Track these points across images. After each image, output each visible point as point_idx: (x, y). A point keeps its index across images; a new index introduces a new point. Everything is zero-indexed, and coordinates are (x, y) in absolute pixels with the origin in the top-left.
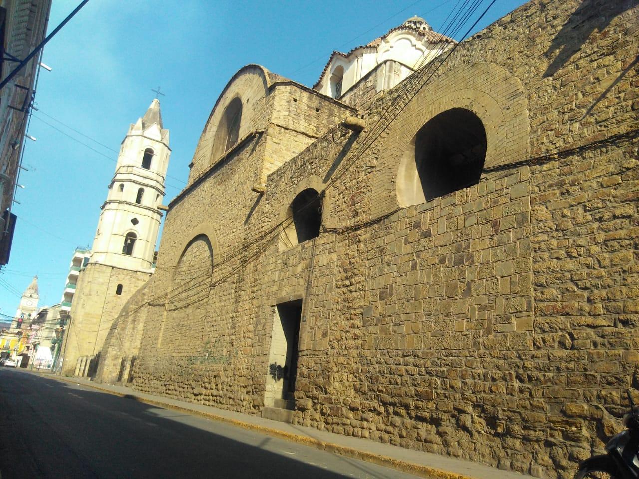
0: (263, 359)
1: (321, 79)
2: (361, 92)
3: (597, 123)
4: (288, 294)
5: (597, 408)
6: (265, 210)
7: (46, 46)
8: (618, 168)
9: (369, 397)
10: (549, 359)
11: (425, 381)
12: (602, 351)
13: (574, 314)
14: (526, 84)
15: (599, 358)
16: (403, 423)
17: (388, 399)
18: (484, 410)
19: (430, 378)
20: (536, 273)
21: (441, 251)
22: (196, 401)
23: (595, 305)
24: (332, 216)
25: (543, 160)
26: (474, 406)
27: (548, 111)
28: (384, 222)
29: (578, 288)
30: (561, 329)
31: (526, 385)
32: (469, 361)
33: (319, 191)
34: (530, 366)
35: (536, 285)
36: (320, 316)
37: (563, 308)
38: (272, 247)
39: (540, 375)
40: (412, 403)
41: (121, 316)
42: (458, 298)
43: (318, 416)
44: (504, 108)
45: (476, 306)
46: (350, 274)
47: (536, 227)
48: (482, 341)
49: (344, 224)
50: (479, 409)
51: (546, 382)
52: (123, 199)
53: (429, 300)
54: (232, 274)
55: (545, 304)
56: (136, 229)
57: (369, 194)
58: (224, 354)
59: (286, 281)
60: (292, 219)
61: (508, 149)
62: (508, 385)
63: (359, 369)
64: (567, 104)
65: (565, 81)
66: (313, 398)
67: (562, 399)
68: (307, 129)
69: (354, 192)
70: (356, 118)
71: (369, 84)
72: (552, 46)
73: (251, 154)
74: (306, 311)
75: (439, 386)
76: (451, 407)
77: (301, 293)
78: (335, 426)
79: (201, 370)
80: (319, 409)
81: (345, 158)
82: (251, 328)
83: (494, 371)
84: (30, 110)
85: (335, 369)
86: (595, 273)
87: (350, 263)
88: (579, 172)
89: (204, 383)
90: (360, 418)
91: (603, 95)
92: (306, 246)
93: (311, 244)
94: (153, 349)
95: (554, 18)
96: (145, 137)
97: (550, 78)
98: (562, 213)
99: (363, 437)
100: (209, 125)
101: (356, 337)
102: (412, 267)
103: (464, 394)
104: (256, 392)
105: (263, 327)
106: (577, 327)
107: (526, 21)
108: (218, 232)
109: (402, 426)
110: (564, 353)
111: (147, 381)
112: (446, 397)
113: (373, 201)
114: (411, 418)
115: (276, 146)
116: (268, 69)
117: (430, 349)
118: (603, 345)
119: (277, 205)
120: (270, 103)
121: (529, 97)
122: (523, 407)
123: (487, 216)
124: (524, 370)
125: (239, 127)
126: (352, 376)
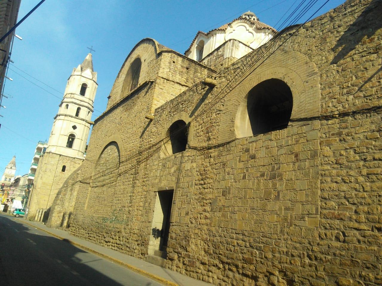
0: (148, 224)
1: (190, 47)
2: (215, 58)
3: (365, 97)
4: (165, 185)
5: (359, 283)
6: (153, 131)
7: (17, 29)
8: (378, 128)
9: (213, 257)
10: (329, 247)
11: (249, 251)
12: (364, 246)
13: (346, 219)
14: (319, 67)
15: (361, 250)
16: (234, 277)
18: (285, 275)
19: (252, 250)
20: (322, 190)
22: (106, 246)
23: (360, 216)
25: (329, 117)
26: (280, 272)
27: (333, 86)
28: (226, 146)
29: (350, 203)
30: (337, 229)
31: (313, 262)
32: (277, 242)
33: (187, 123)
34: (316, 250)
35: (322, 198)
36: (184, 201)
37: (339, 215)
38: (156, 155)
39: (323, 256)
40: (240, 265)
41: (63, 187)
42: (271, 200)
43: (181, 265)
44: (305, 82)
45: (283, 208)
47: (323, 160)
48: (286, 230)
49: (202, 145)
50: (283, 273)
51: (326, 262)
52: (68, 113)
53: (253, 199)
54: (131, 169)
55: (327, 211)
56: (75, 132)
57: (217, 127)
58: (124, 219)
59: (164, 177)
60: (169, 138)
61: (306, 108)
62: (301, 261)
63: (207, 238)
64: (346, 83)
65: (345, 68)
66: (178, 253)
67: (337, 274)
68: (180, 80)
69: (209, 125)
70: (211, 79)
71: (220, 53)
72: (337, 44)
74: (176, 197)
75: (258, 256)
76: (265, 270)
77: (173, 185)
78: (191, 273)
79: (110, 227)
80: (182, 261)
81: (203, 103)
82: (141, 204)
83: (293, 251)
84: (8, 65)
85: (193, 236)
86: (360, 194)
87: (205, 170)
88: (352, 128)
89: (112, 235)
90: (207, 270)
91: (370, 80)
92: (177, 157)
93: (180, 155)
94: (81, 210)
95: (339, 27)
96: (82, 76)
97: (335, 65)
98: (340, 153)
99: (208, 282)
100: (121, 73)
101: (206, 218)
102: (243, 177)
103: (273, 263)
104: (143, 245)
105: (149, 204)
106: (348, 229)
107: (321, 27)
108: (124, 141)
109: (233, 279)
110: (338, 244)
111: (77, 229)
112: (262, 263)
113: (220, 132)
114: (239, 274)
116: (158, 41)
117: (253, 231)
118: (365, 242)
120: (159, 63)
121: (321, 76)
122: (311, 276)
123: (292, 150)
124: (312, 252)
125: (139, 76)
126: (203, 242)
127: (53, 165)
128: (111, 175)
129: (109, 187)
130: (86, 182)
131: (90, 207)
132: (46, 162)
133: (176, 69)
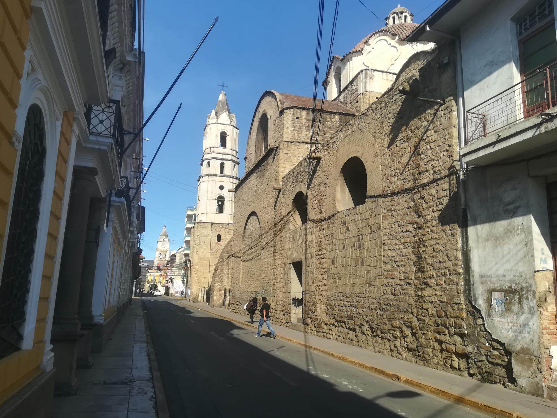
0: (288, 295)
17: (339, 319)
21: (353, 240)
40: (346, 321)
41: (219, 262)
43: (313, 328)
48: (368, 289)
52: (212, 172)
57: (326, 200)
66: (311, 318)
71: (354, 88)
73: (273, 161)
82: (282, 276)
85: (318, 302)
115: (286, 155)
119: (287, 199)
127: (207, 236)
130: (238, 256)
131: (244, 282)
132: (199, 234)
133: (301, 125)
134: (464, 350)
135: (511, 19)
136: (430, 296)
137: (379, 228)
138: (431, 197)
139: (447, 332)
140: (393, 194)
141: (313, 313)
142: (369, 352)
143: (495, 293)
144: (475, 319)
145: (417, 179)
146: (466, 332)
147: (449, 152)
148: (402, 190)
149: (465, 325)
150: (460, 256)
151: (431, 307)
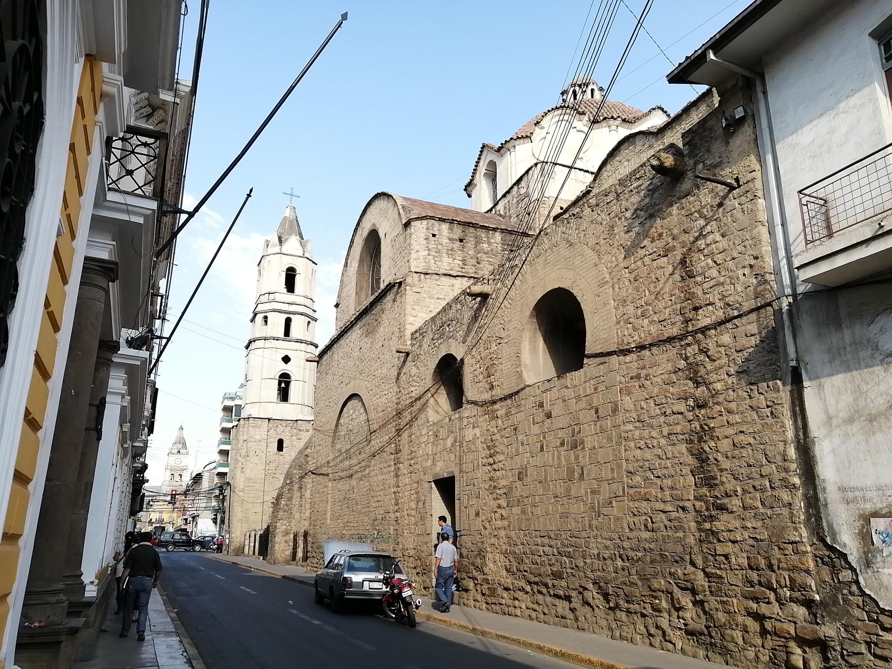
0: (427, 539)
4: (442, 470)
17: (533, 579)
24: (472, 390)
38: (423, 416)
40: (550, 583)
41: (285, 484)
43: (479, 597)
46: (492, 451)
48: (594, 522)
51: (638, 561)
52: (269, 335)
55: (634, 490)
56: (288, 368)
57: (500, 367)
59: (438, 455)
66: (474, 579)
71: (522, 191)
85: (489, 549)
95: (626, 210)
101: (502, 518)
114: (550, 596)
119: (423, 369)
126: (502, 556)
128: (360, 457)
129: (361, 480)
131: (336, 518)
132: (245, 438)
133: (440, 247)
134: (815, 632)
135: (869, 35)
136: (731, 531)
137: (615, 410)
138: (722, 349)
139: (772, 596)
140: (641, 347)
141: (480, 570)
142: (602, 638)
143: (878, 519)
144: (834, 571)
145: (691, 320)
146: (817, 597)
147: (756, 268)
148: (661, 341)
149: (813, 584)
150: (792, 452)
151: (735, 550)
